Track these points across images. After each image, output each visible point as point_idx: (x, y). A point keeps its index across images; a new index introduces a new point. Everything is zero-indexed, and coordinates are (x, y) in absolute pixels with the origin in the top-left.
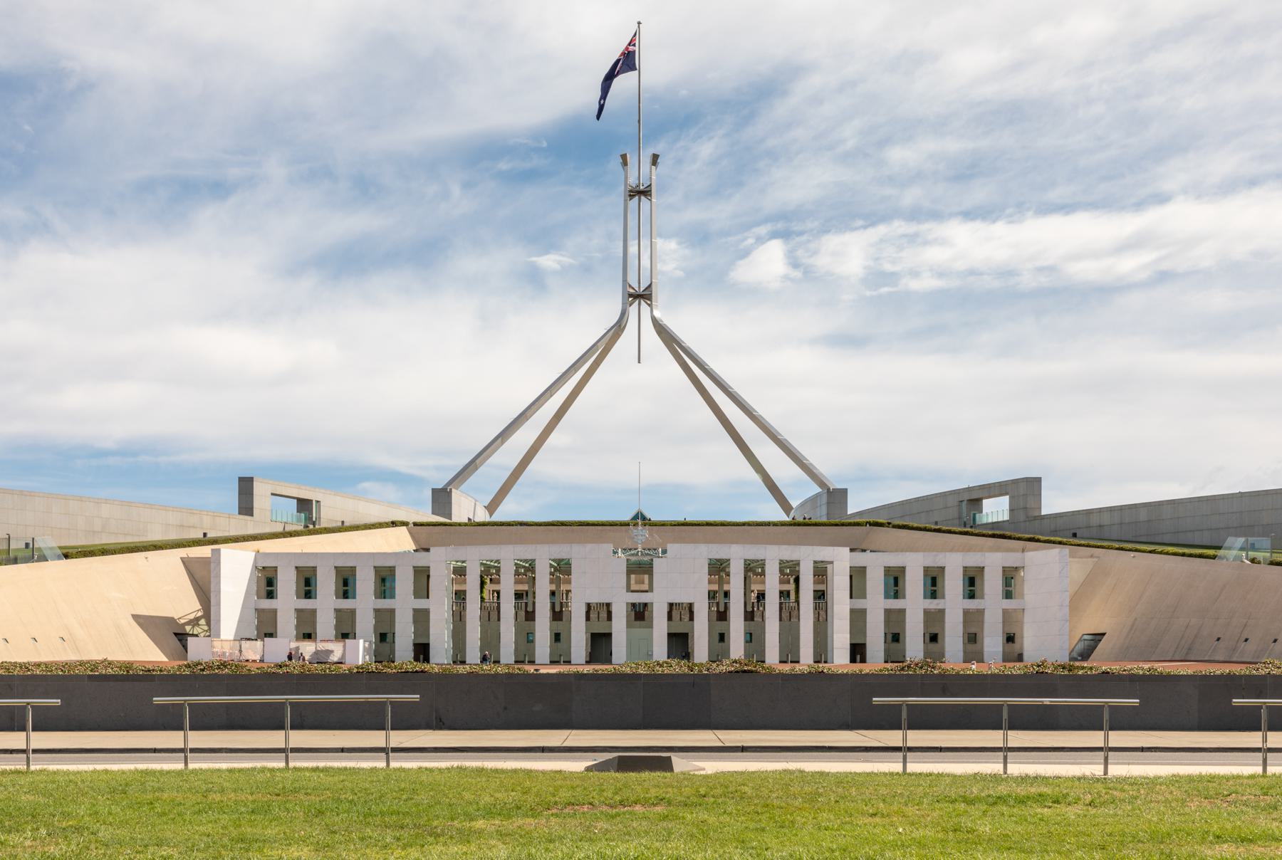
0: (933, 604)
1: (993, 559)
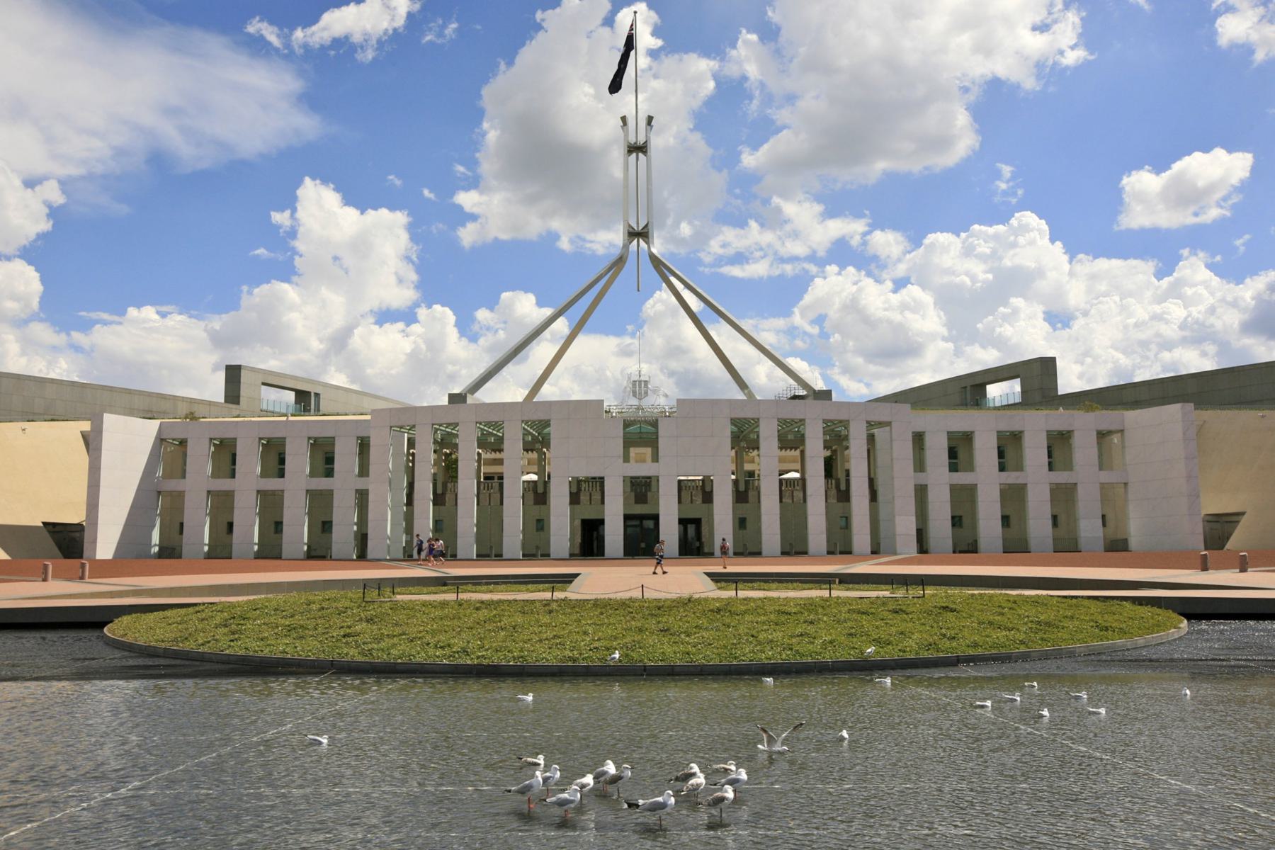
0: (1011, 477)
1: (1084, 424)
